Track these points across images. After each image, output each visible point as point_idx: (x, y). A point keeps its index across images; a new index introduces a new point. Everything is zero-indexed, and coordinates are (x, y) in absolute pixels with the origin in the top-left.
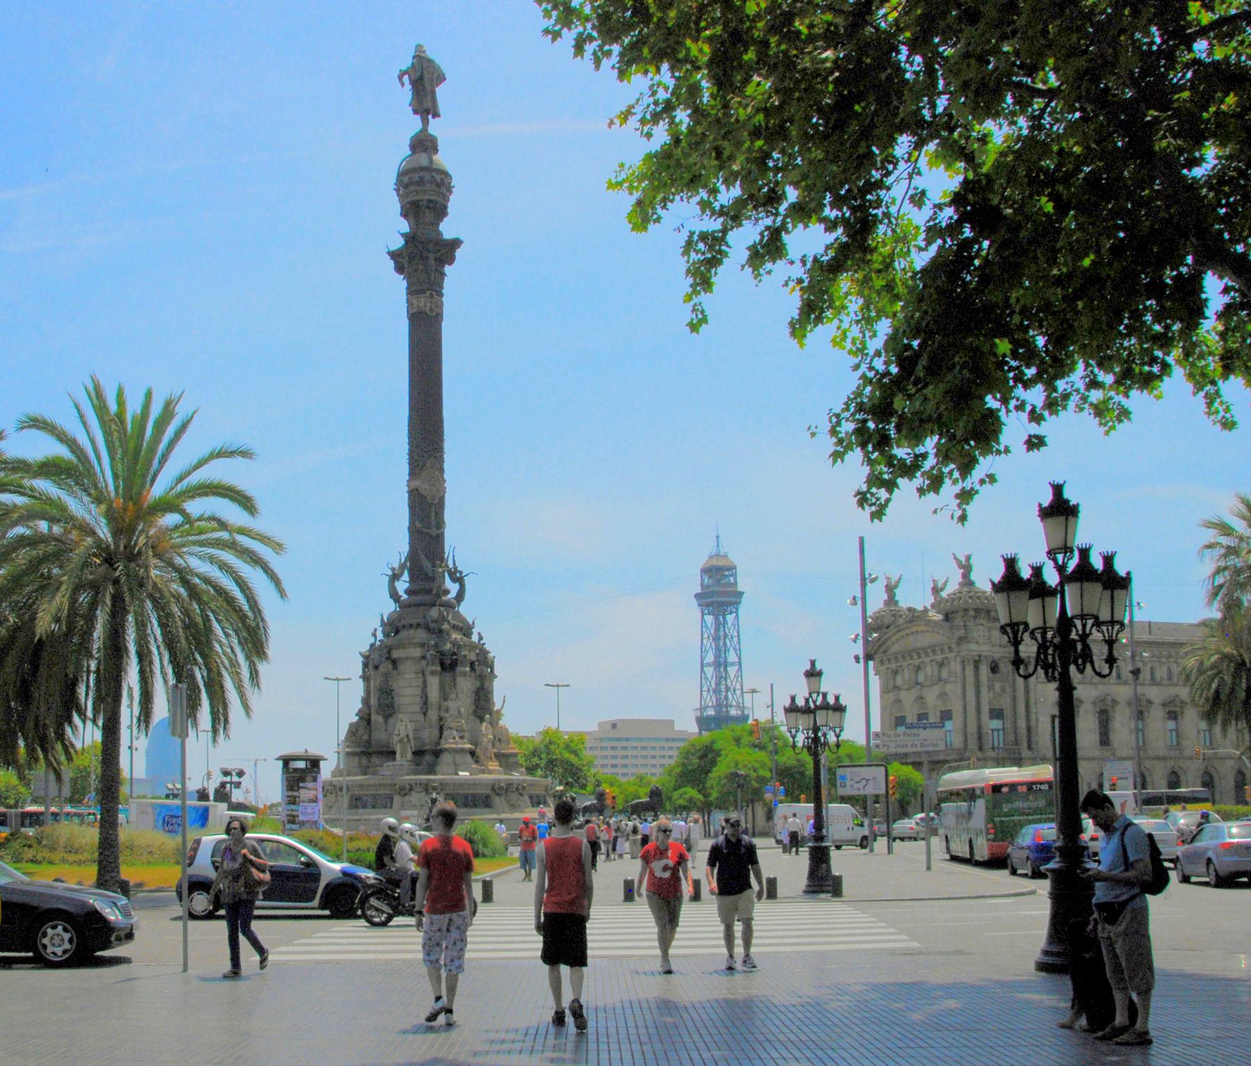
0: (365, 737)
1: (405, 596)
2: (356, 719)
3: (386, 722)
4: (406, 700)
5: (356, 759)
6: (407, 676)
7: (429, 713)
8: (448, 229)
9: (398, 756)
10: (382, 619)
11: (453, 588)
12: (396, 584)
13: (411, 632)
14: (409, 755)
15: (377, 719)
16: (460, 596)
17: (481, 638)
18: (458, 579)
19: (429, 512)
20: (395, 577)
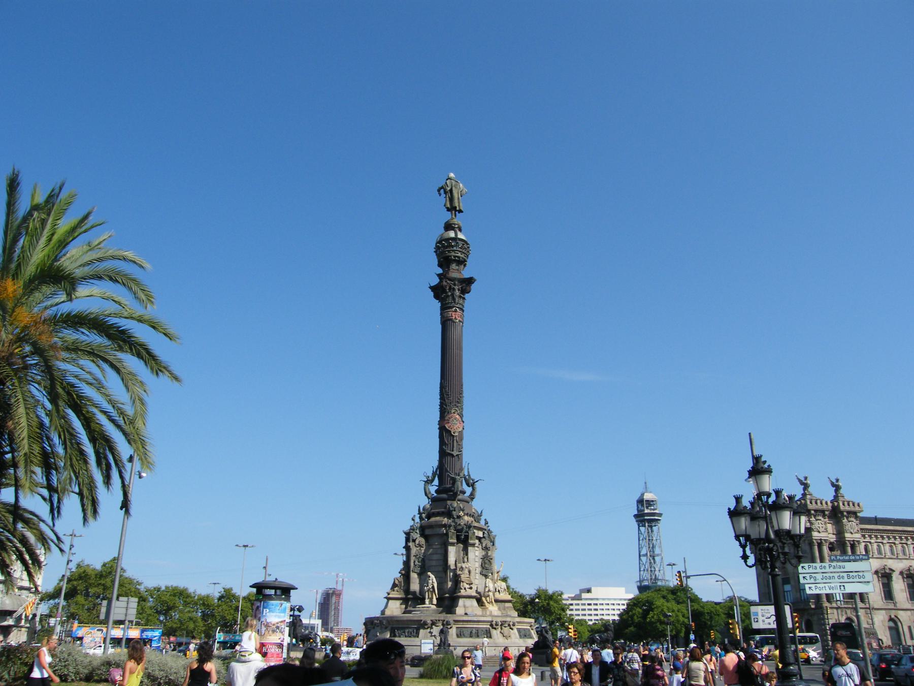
4: (434, 563)
8: (466, 273)
9: (427, 601)
13: (438, 518)
14: (435, 601)
16: (472, 496)
17: (486, 523)
18: (472, 484)
20: (429, 482)
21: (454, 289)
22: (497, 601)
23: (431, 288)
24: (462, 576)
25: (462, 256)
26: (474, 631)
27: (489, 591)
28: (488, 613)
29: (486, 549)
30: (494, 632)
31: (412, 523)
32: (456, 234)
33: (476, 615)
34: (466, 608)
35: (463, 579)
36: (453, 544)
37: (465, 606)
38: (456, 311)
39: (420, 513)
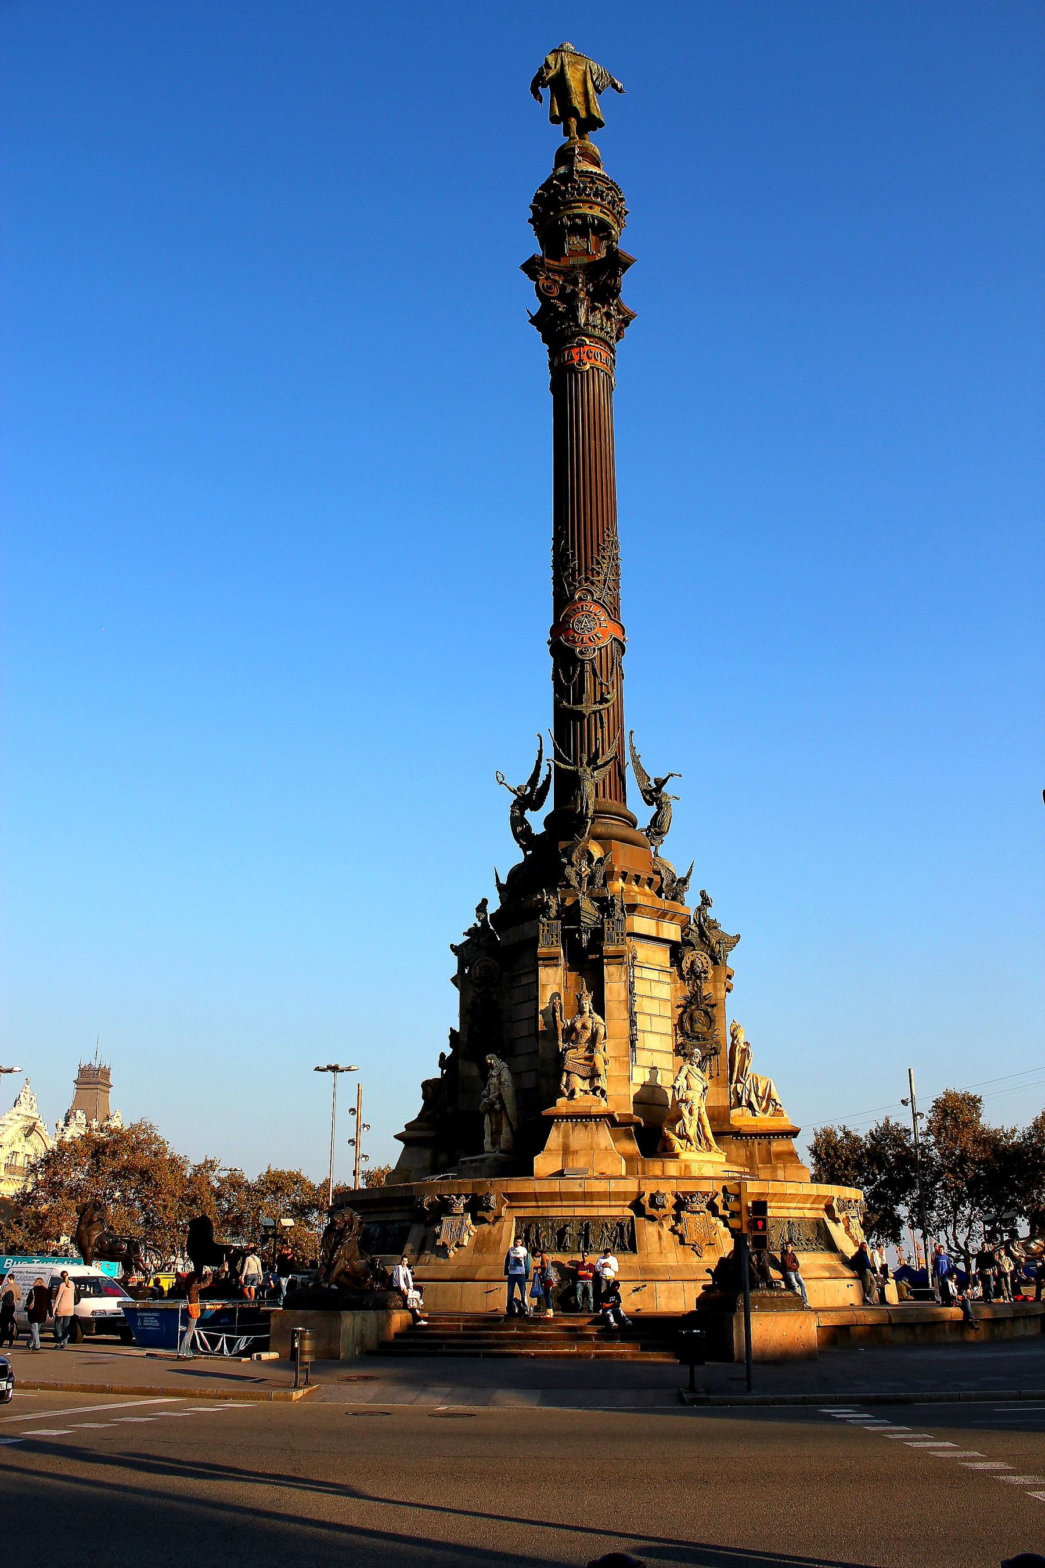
11: (643, 814)
12: (529, 814)
17: (706, 902)
21: (574, 295)
24: (570, 1054)
25: (596, 212)
29: (694, 975)
30: (648, 1232)
33: (603, 1176)
36: (551, 960)
37: (566, 1151)
38: (582, 344)
39: (500, 888)
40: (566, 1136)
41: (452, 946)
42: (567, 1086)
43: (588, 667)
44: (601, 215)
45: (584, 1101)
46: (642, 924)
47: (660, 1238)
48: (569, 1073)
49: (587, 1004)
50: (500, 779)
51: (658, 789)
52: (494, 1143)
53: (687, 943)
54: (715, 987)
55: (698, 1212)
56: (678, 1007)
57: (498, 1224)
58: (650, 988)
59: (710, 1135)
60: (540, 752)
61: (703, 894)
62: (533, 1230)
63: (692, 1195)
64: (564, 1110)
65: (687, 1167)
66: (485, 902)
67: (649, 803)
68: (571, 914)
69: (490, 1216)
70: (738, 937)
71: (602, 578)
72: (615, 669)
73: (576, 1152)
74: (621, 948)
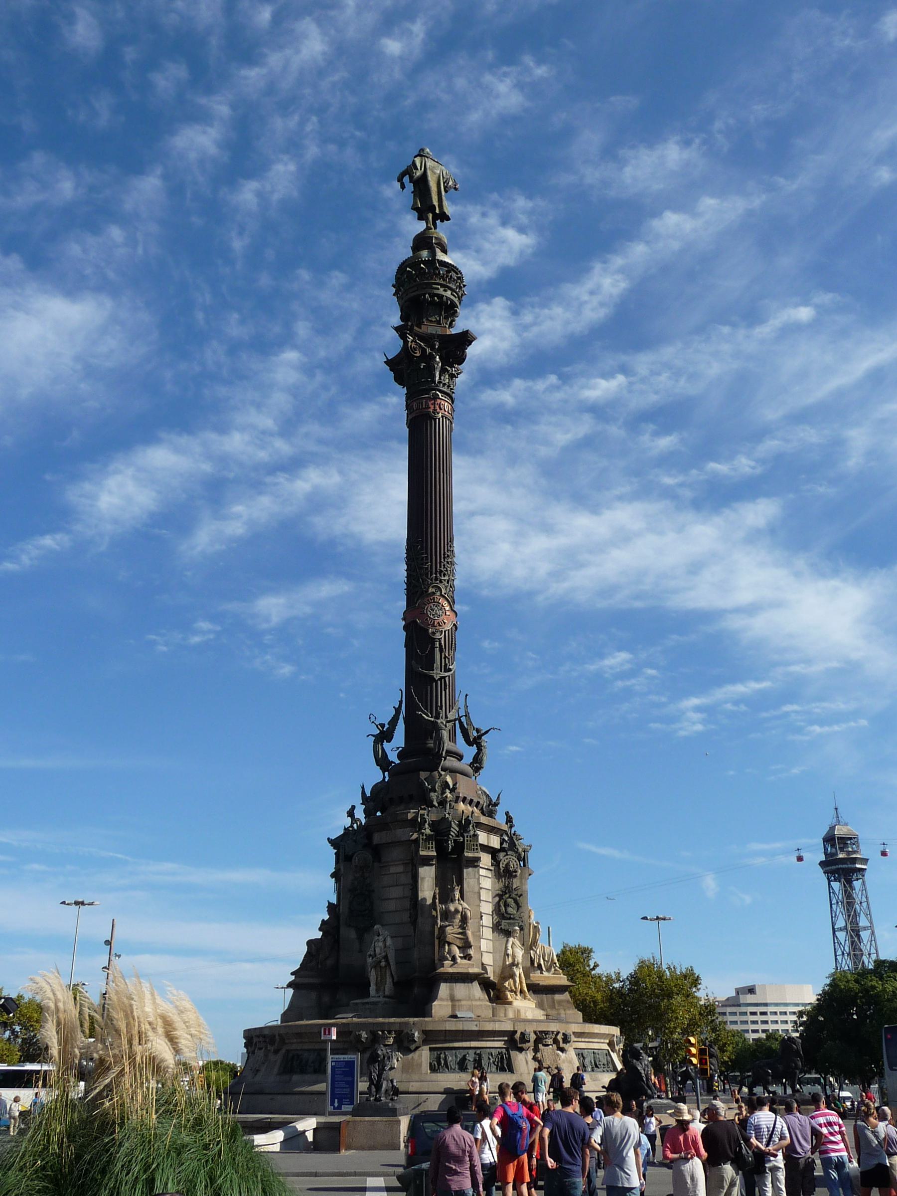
0: (330, 962)
1: (398, 762)
2: (319, 935)
3: (360, 938)
4: (391, 906)
5: (313, 995)
6: (393, 870)
7: (420, 920)
9: (373, 988)
10: (363, 793)
15: (349, 934)
16: (477, 764)
17: (509, 820)
19: (433, 648)
20: (385, 735)
22: (535, 989)
23: (388, 362)
24: (449, 929)
26: (471, 1057)
27: (514, 964)
28: (511, 1015)
31: (348, 822)
32: (434, 254)
34: (456, 1005)
35: (449, 938)
36: (426, 861)
37: (452, 999)
38: (436, 397)
39: (365, 800)
40: (452, 989)
41: (328, 839)
42: (449, 952)
43: (437, 644)
44: (452, 297)
45: (463, 967)
46: (483, 838)
47: (527, 1063)
48: (449, 944)
49: (457, 895)
50: (373, 719)
51: (480, 737)
52: (377, 991)
53: (502, 849)
54: (521, 882)
55: (548, 1045)
56: (498, 895)
57: (417, 1052)
58: (483, 882)
59: (525, 989)
60: (401, 702)
61: (507, 813)
62: (442, 1056)
63: (546, 1033)
64: (451, 970)
65: (519, 1011)
66: (353, 807)
67: (470, 743)
68: (440, 829)
69: (413, 1047)
70: (530, 846)
71: (446, 578)
72: (452, 646)
73: (459, 1000)
74: (476, 855)
